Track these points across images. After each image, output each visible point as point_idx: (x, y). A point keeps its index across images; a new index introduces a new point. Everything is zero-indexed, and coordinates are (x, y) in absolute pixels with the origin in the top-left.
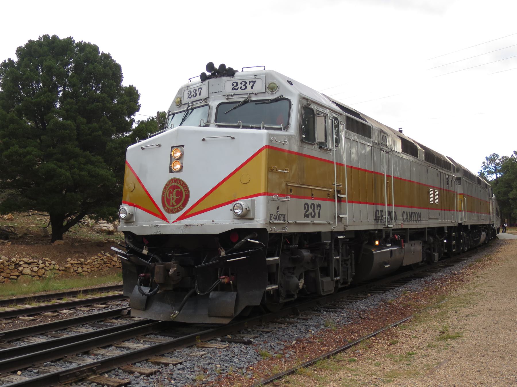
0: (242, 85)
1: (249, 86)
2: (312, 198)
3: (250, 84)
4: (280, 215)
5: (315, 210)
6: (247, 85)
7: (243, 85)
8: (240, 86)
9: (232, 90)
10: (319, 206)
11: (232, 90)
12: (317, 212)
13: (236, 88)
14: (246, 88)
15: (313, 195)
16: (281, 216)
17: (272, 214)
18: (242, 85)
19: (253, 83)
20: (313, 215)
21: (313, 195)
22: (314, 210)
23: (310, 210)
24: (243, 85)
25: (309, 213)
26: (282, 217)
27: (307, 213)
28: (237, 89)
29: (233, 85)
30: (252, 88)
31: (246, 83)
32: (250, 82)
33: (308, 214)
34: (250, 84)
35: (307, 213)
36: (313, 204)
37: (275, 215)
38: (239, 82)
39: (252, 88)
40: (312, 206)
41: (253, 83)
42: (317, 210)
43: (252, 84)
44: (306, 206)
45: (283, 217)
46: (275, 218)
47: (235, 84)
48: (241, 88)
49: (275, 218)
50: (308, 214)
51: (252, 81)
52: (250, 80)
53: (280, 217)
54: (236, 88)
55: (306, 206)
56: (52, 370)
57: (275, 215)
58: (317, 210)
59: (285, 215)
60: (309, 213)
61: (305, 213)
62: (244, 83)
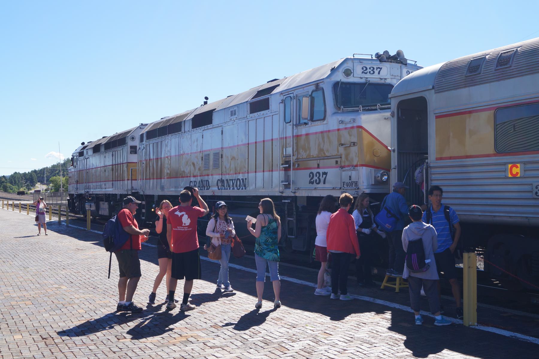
0: (370, 70)
1: (376, 72)
2: (318, 167)
3: (377, 70)
4: (352, 182)
5: (321, 177)
6: (375, 70)
7: (372, 70)
8: (368, 70)
9: (362, 73)
10: (325, 173)
11: (362, 73)
12: (322, 179)
13: (366, 72)
14: (374, 72)
15: (318, 165)
16: (353, 182)
17: (345, 182)
18: (370, 70)
19: (380, 69)
20: (317, 182)
21: (318, 165)
22: (319, 178)
23: (315, 178)
24: (372, 70)
25: (314, 180)
26: (354, 184)
27: (312, 180)
28: (366, 73)
29: (363, 69)
30: (379, 73)
31: (374, 68)
32: (377, 68)
33: (313, 181)
34: (377, 70)
35: (312, 180)
36: (319, 173)
37: (347, 183)
38: (368, 67)
39: (379, 73)
40: (318, 174)
41: (380, 69)
42: (323, 177)
43: (379, 70)
44: (311, 175)
45: (355, 184)
46: (347, 185)
47: (365, 69)
48: (370, 72)
49: (347, 185)
50: (313, 181)
51: (379, 68)
52: (378, 67)
53: (352, 184)
54: (366, 72)
55: (311, 175)
56: (358, 342)
57: (347, 183)
58: (323, 177)
59: (357, 182)
60: (314, 180)
61: (310, 181)
62: (372, 69)
